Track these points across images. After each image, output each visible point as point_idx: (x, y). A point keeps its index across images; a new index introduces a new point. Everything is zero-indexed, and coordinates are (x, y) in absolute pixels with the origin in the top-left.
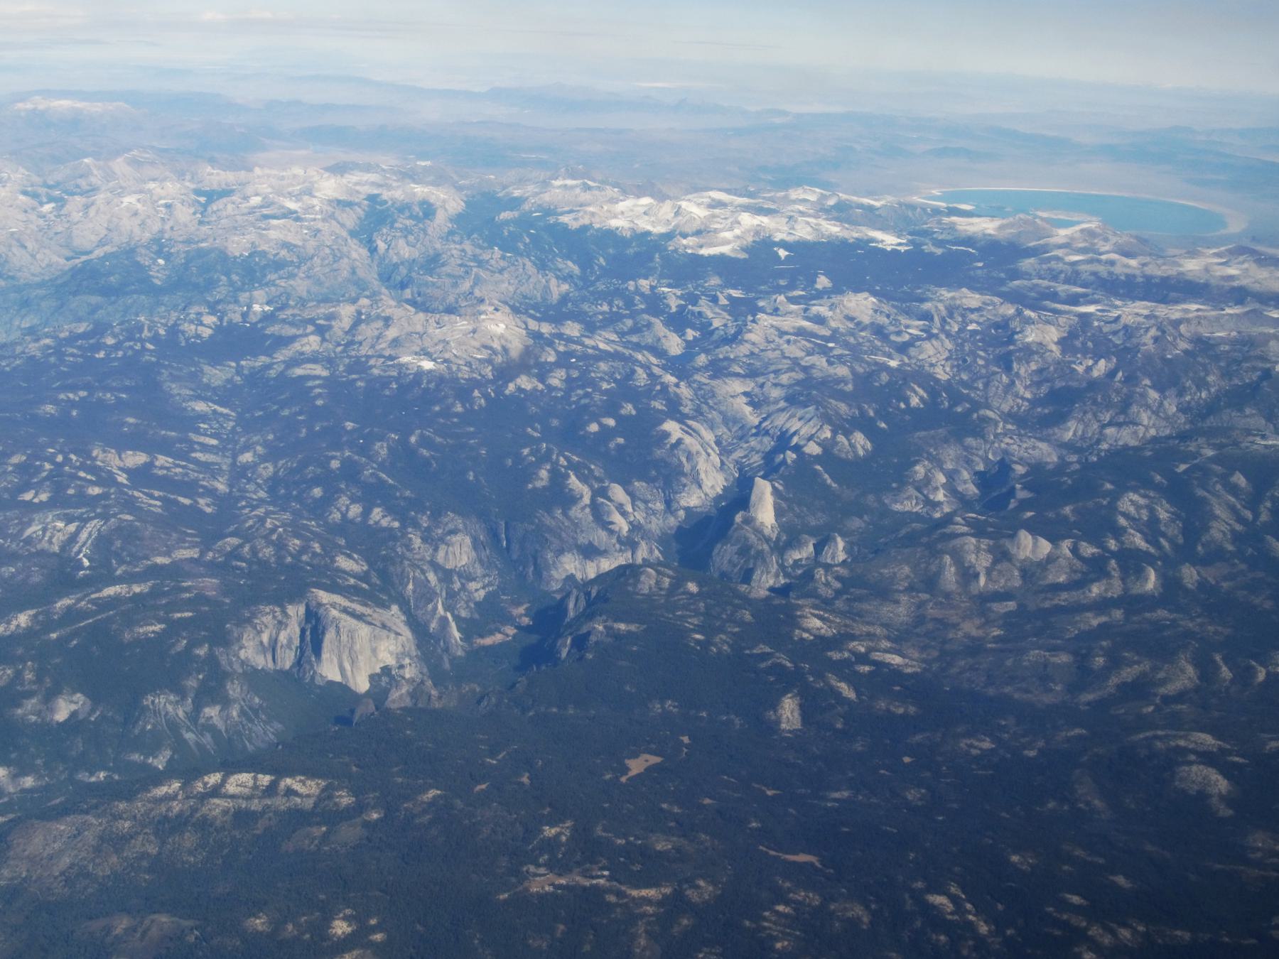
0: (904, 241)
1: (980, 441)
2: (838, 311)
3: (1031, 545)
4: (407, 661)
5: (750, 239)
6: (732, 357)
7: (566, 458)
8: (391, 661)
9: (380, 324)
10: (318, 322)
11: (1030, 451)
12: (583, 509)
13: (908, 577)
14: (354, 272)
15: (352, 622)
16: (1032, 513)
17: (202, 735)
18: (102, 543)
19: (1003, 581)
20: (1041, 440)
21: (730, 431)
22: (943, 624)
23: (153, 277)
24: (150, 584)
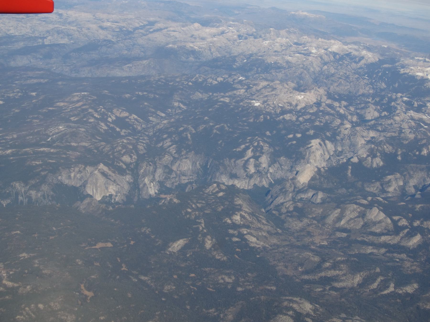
3: (375, 215)
4: (119, 194)
6: (383, 124)
9: (270, 90)
10: (250, 85)
13: (319, 213)
14: (301, 74)
15: (99, 176)
16: (405, 204)
17: (25, 199)
18: (65, 134)
19: (352, 225)
21: (350, 148)
22: (309, 234)
23: (235, 65)
24: (58, 150)
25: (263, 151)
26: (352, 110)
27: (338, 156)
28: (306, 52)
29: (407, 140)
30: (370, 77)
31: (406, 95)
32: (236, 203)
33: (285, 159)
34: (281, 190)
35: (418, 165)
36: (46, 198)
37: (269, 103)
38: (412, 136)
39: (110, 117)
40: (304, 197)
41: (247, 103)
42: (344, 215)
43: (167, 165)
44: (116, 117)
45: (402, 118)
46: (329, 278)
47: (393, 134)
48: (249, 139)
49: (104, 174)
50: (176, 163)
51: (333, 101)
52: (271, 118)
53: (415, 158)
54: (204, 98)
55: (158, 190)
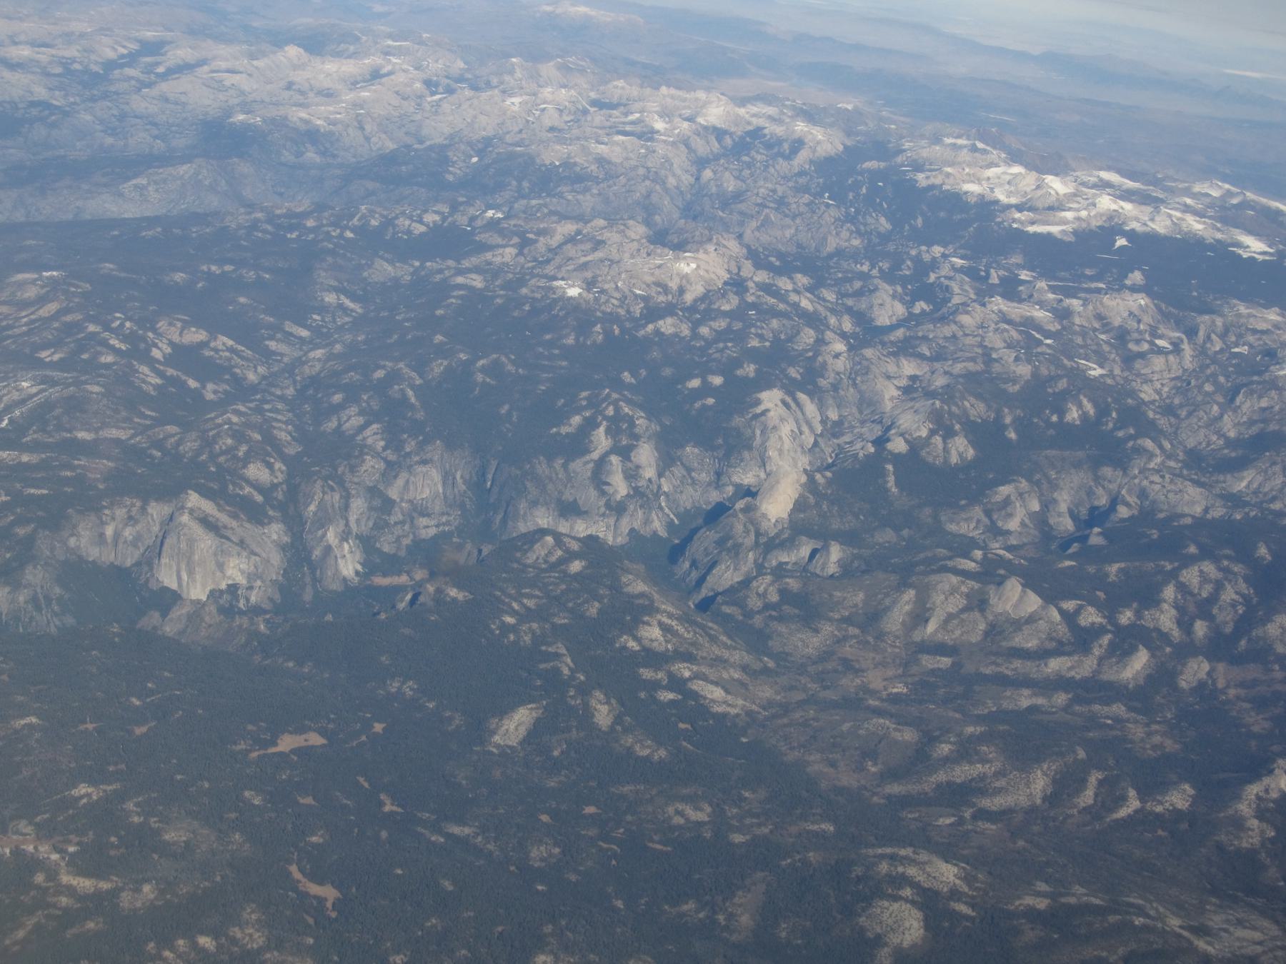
0: (1271, 251)
1: (1119, 473)
2: (1090, 307)
4: (259, 583)
5: (1095, 223)
6: (931, 336)
7: (617, 409)
8: (241, 579)
9: (588, 246)
11: (1171, 495)
12: (586, 463)
13: (856, 606)
14: (648, 196)
15: (198, 530)
18: (48, 406)
19: (958, 633)
20: (1197, 483)
21: (861, 412)
22: (848, 666)
23: (450, 173)
24: (43, 456)
25: (637, 430)
26: (829, 298)
27: (835, 436)
28: (638, 129)
29: (1014, 381)
30: (839, 198)
31: (955, 251)
32: (629, 589)
33: (696, 450)
34: (721, 543)
35: (1067, 453)
36: (43, 606)
37: (606, 286)
38: (1024, 370)
39: (156, 346)
40: (787, 560)
41: (542, 288)
42: (928, 606)
43: (375, 486)
44: (171, 343)
45: (978, 318)
46: (962, 785)
47: (971, 366)
48: (585, 398)
49: (207, 523)
50: (395, 477)
51: (771, 275)
52: (623, 331)
53: (1051, 432)
54: (402, 276)
55: (360, 563)
